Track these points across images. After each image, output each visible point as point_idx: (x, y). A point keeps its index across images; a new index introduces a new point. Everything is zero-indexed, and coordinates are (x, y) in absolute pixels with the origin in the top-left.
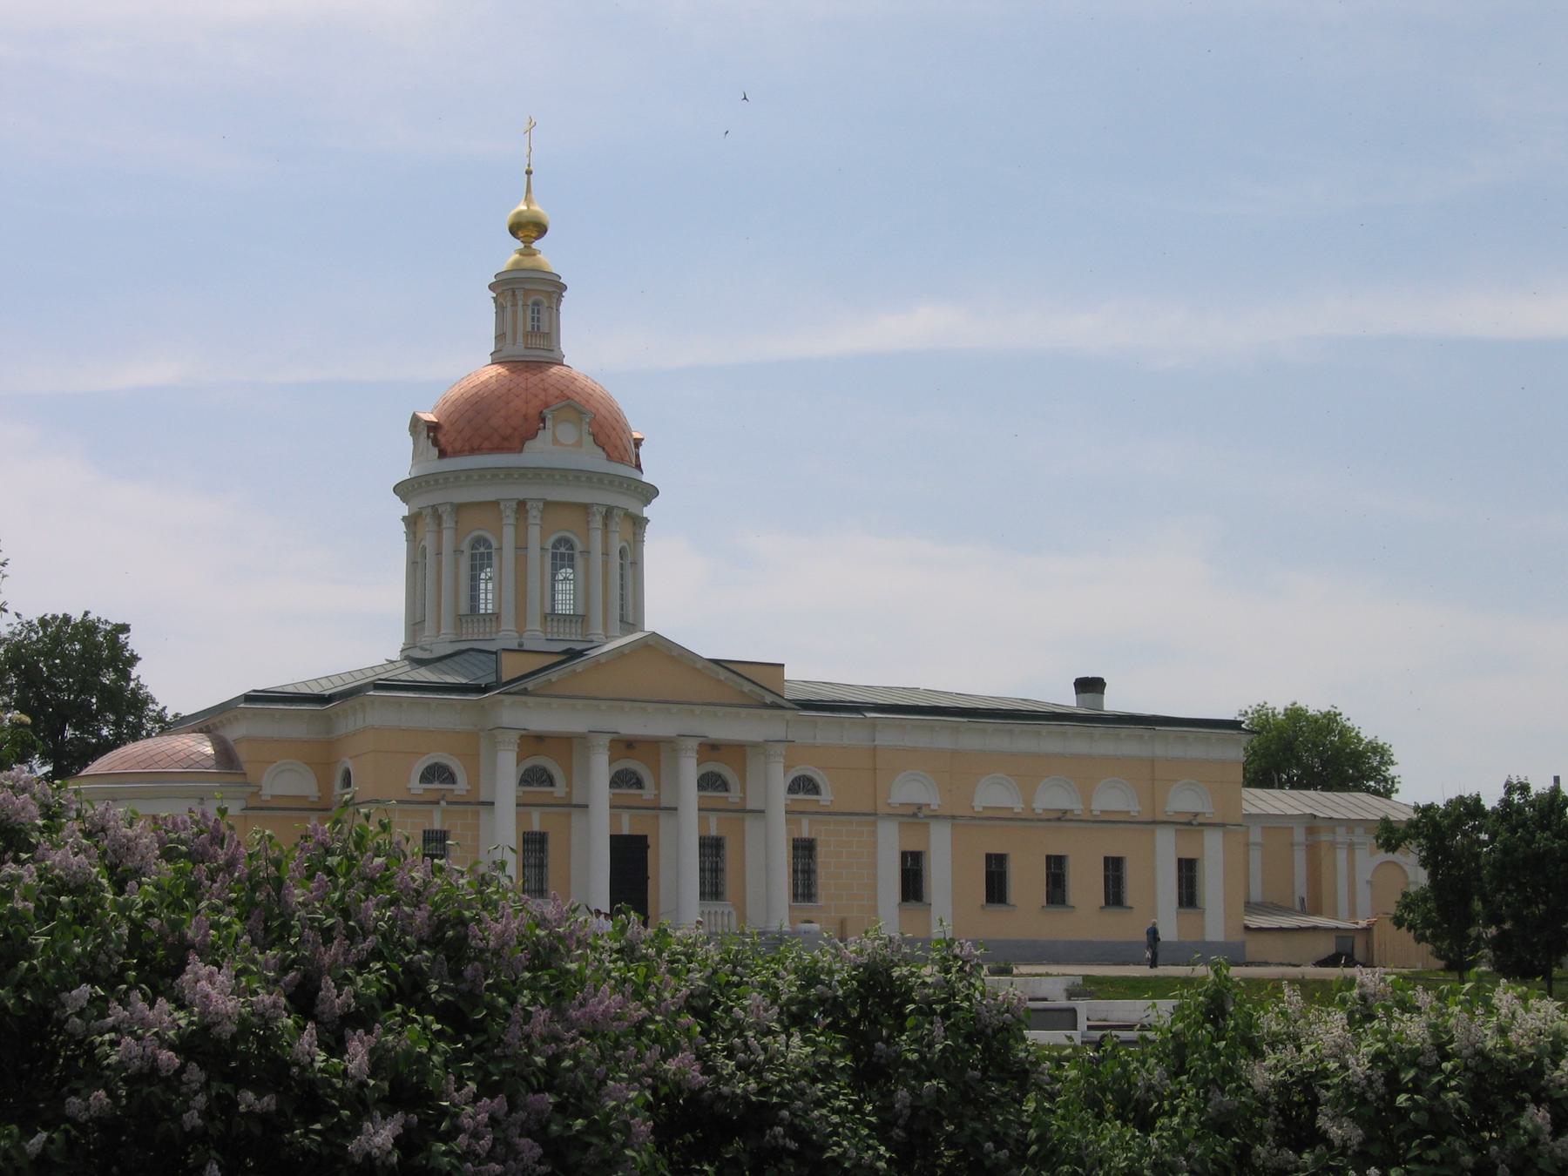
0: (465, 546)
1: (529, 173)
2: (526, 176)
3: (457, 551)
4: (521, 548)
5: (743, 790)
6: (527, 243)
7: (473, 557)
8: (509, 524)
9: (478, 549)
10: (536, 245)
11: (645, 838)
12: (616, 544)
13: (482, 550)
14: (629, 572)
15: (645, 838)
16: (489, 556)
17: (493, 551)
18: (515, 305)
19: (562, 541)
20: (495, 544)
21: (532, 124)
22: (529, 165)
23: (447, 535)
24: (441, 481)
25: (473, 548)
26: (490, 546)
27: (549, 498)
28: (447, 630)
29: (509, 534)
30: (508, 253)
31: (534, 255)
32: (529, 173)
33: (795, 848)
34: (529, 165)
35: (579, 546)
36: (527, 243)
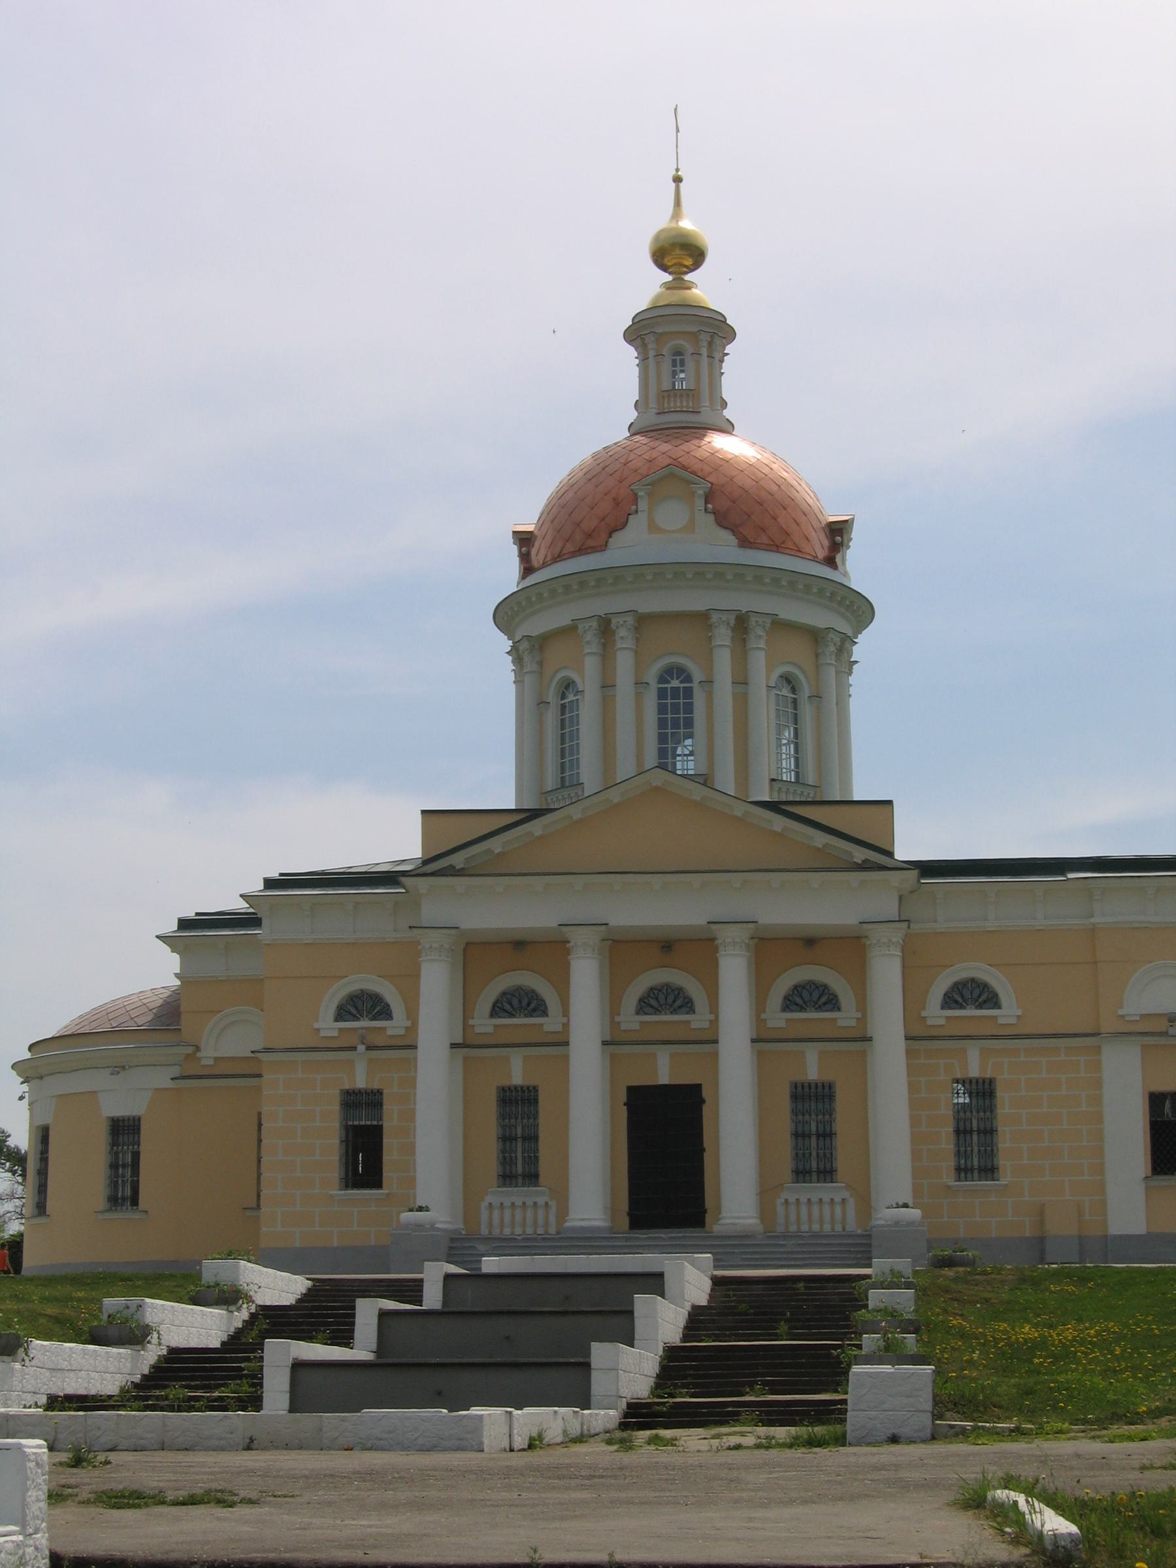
0: (651, 676)
1: (678, 180)
2: (674, 185)
3: (640, 684)
5: (566, 1013)
7: (662, 693)
8: (726, 646)
9: (668, 682)
11: (698, 1087)
13: (675, 683)
15: (698, 1087)
16: (689, 693)
17: (695, 685)
20: (698, 675)
22: (677, 170)
24: (575, 587)
25: (662, 679)
26: (689, 679)
27: (782, 616)
29: (723, 662)
31: (689, 288)
32: (678, 180)
33: (795, 1097)
34: (677, 170)
35: (806, 691)
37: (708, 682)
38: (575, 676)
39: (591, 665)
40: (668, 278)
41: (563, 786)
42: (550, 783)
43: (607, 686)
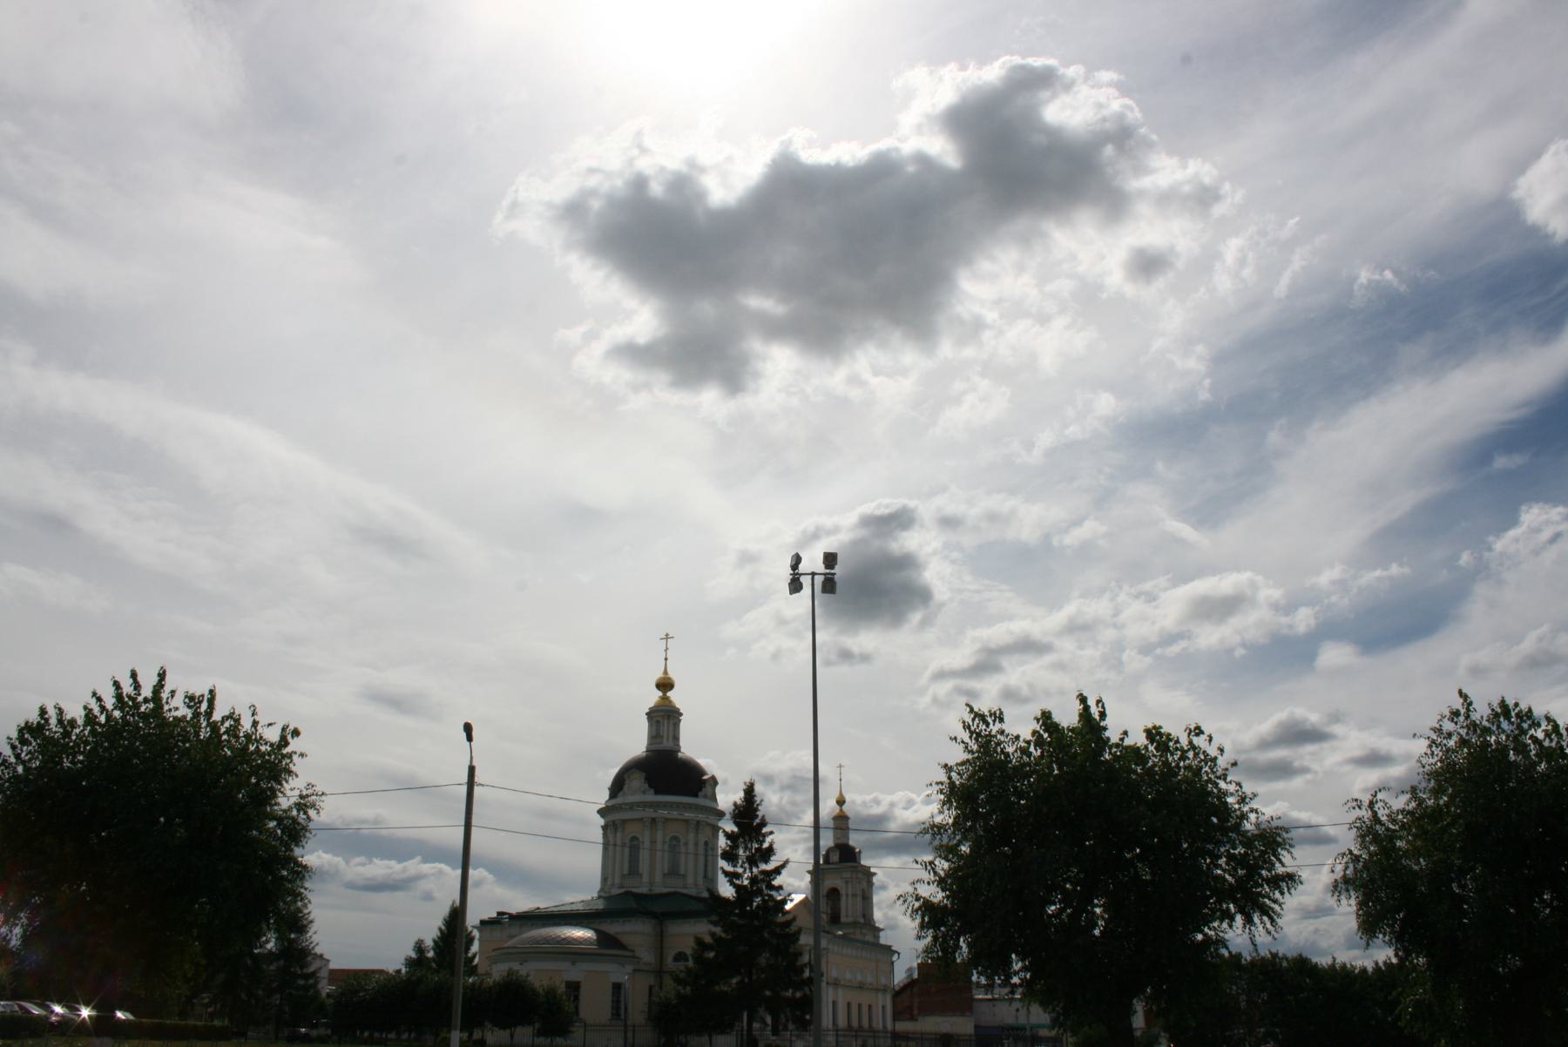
1: (666, 659)
3: (664, 842)
4: (696, 844)
6: (665, 693)
10: (669, 694)
12: (702, 839)
14: (710, 858)
18: (668, 723)
19: (675, 838)
20: (683, 841)
21: (667, 637)
23: (659, 835)
28: (658, 878)
30: (655, 696)
32: (666, 659)
35: (710, 846)
36: (665, 693)
37: (686, 844)
38: (637, 835)
39: (647, 833)
40: (661, 694)
41: (629, 874)
42: (626, 872)
43: (653, 842)
